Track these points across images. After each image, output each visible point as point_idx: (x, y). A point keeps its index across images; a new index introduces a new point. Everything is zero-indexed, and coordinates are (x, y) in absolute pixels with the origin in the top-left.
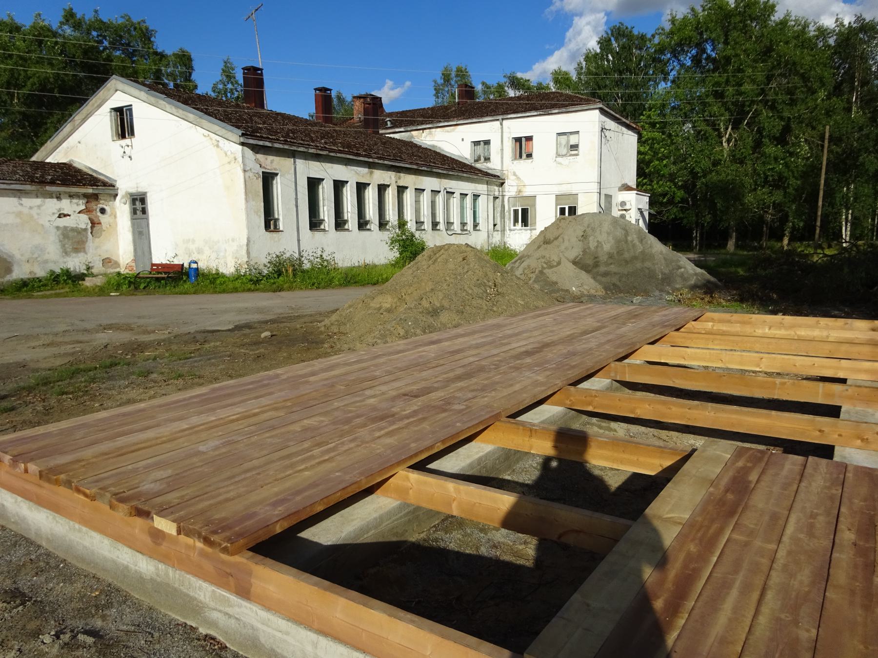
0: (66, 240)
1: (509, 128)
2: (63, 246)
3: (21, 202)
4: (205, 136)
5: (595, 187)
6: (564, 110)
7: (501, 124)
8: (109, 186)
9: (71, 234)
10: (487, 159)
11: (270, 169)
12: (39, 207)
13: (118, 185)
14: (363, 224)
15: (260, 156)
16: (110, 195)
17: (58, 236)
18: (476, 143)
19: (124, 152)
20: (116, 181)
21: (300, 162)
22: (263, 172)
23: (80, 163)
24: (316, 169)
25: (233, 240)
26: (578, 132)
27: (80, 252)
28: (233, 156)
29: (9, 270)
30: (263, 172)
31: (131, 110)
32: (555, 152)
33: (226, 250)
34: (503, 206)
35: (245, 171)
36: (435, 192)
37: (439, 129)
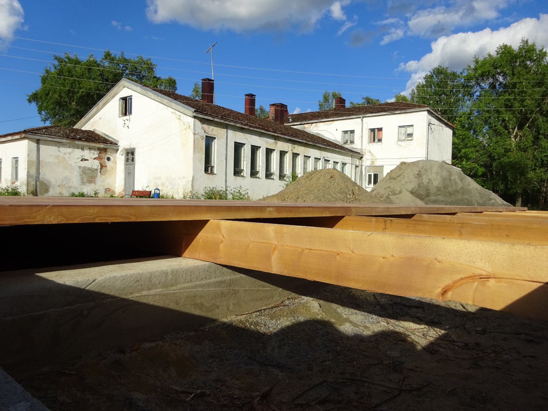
0: (84, 175)
1: (366, 122)
2: (82, 178)
3: (59, 150)
4: (173, 113)
6: (403, 111)
7: (362, 120)
8: (114, 144)
9: (87, 172)
10: (352, 142)
12: (70, 153)
13: (119, 144)
14: (268, 175)
15: (205, 126)
17: (80, 172)
18: (345, 132)
19: (125, 123)
20: (118, 141)
21: (230, 132)
22: (206, 136)
23: (99, 131)
24: (240, 137)
25: (184, 178)
26: (412, 126)
27: (92, 183)
28: (188, 125)
29: (47, 191)
30: (206, 136)
31: (131, 99)
32: (397, 138)
33: (179, 184)
34: (361, 172)
35: (194, 134)
36: (317, 159)
37: (322, 123)
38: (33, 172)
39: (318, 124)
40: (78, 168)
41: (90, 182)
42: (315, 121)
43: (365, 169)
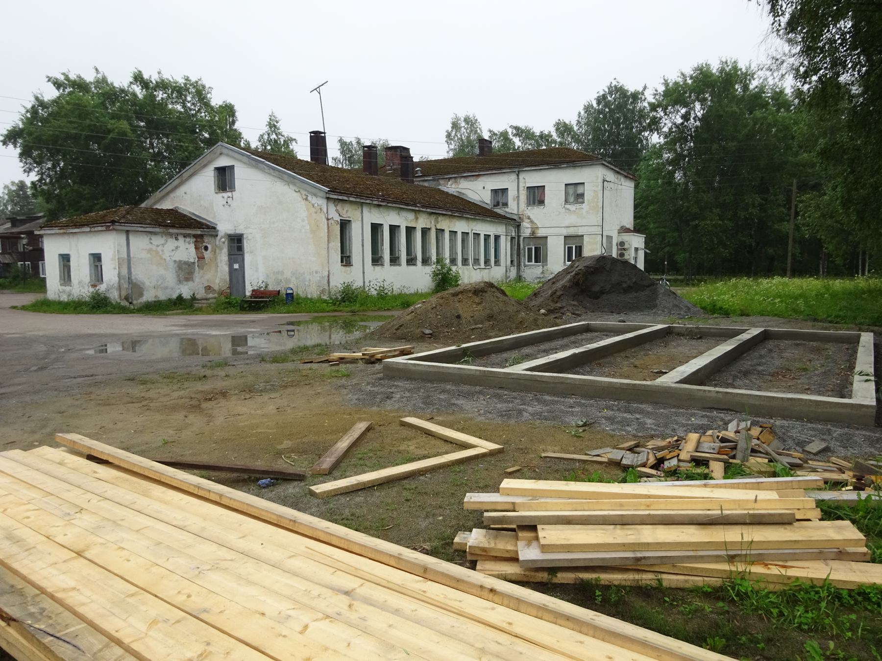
2: (178, 276)
5: (598, 230)
7: (518, 176)
9: (184, 266)
10: (506, 205)
11: (345, 217)
13: (219, 227)
14: (411, 261)
16: (212, 236)
18: (495, 192)
21: (366, 210)
23: (184, 210)
25: (316, 272)
28: (319, 207)
29: (141, 295)
35: (328, 219)
37: (462, 179)
38: (125, 272)
39: (458, 179)
40: (173, 263)
41: (188, 279)
42: (453, 176)
43: (524, 241)
